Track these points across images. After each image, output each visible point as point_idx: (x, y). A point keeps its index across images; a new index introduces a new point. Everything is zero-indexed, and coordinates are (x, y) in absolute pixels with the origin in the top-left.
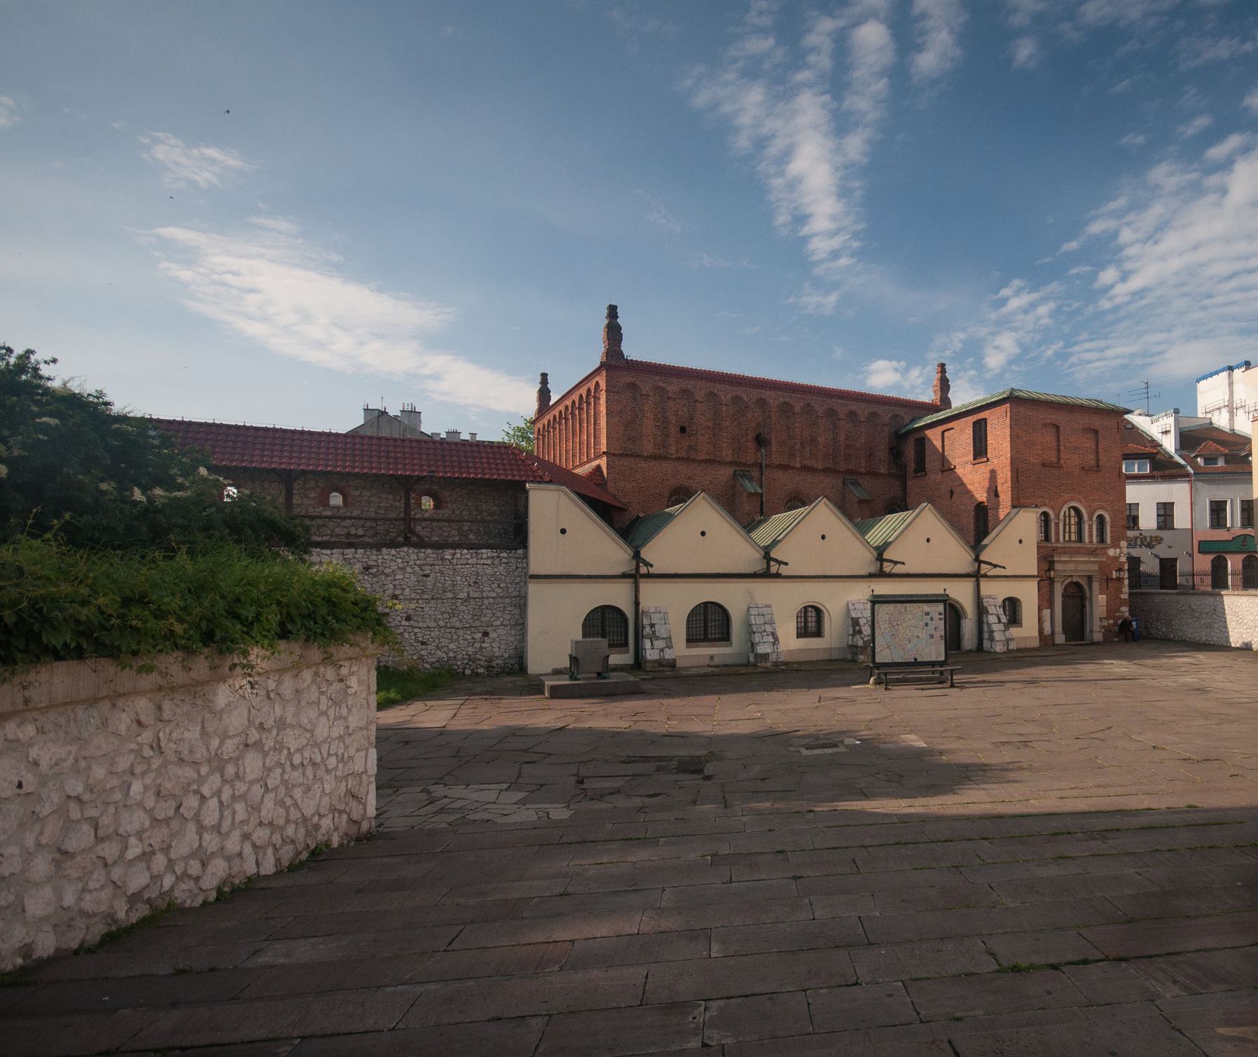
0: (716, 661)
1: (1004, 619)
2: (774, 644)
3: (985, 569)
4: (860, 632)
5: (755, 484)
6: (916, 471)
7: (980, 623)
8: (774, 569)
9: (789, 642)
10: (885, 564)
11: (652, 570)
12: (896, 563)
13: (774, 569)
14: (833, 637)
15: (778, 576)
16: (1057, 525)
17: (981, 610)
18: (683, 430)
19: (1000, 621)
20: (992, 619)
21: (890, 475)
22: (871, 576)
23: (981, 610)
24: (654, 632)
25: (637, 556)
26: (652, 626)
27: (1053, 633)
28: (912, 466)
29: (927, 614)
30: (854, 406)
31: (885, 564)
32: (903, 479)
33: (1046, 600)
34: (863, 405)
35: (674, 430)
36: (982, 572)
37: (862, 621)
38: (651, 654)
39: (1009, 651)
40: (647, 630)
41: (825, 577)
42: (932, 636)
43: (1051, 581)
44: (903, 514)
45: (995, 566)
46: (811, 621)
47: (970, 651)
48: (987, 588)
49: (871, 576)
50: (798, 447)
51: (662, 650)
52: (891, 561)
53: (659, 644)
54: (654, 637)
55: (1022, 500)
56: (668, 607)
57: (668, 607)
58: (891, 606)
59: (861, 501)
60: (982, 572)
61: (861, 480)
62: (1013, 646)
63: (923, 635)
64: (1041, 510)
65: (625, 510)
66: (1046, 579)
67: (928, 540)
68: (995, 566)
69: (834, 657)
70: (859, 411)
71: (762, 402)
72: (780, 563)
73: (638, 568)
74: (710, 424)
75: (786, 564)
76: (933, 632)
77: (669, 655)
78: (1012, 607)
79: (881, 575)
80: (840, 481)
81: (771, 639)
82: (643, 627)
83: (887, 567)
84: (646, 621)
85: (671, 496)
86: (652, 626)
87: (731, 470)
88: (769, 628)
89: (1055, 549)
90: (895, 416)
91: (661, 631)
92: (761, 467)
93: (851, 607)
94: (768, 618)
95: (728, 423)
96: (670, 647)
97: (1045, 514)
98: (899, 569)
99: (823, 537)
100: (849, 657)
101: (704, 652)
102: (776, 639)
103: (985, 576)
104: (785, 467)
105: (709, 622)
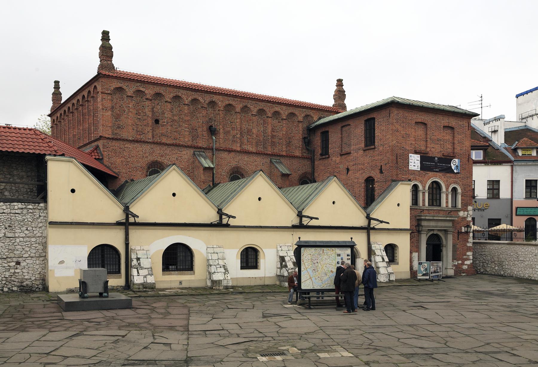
0: (184, 285)
1: (386, 259)
2: (225, 274)
3: (373, 223)
4: (286, 266)
5: (208, 161)
6: (322, 155)
8: (225, 221)
9: (236, 273)
10: (304, 219)
11: (138, 220)
12: (312, 218)
13: (225, 221)
14: (268, 268)
15: (227, 226)
16: (424, 193)
17: (370, 252)
18: (157, 122)
20: (378, 259)
21: (303, 158)
23: (370, 252)
24: (139, 264)
25: (126, 210)
26: (138, 259)
28: (319, 151)
29: (339, 255)
30: (277, 108)
31: (304, 219)
32: (312, 160)
33: (415, 247)
34: (284, 108)
35: (150, 122)
36: (372, 226)
37: (287, 259)
38: (137, 279)
40: (135, 262)
41: (261, 227)
43: (419, 232)
44: (310, 185)
45: (382, 222)
46: (250, 258)
49: (294, 227)
50: (238, 136)
51: (145, 277)
52: (308, 217)
53: (143, 272)
54: (139, 267)
56: (149, 249)
57: (149, 249)
59: (284, 175)
60: (372, 226)
61: (282, 160)
62: (393, 278)
65: (116, 178)
66: (416, 229)
67: (334, 203)
68: (382, 222)
69: (266, 283)
70: (281, 112)
71: (212, 104)
72: (230, 217)
73: (127, 218)
74: (175, 118)
75: (234, 217)
77: (150, 280)
78: (391, 249)
79: (300, 226)
80: (269, 162)
81: (222, 270)
82: (132, 260)
83: (305, 221)
84: (133, 256)
85: (149, 168)
86: (138, 259)
87: (192, 151)
88: (221, 263)
89: (423, 210)
90: (307, 116)
91: (145, 263)
92: (212, 149)
93: (279, 249)
94: (220, 255)
95: (189, 118)
96: (151, 275)
97: (415, 188)
98: (313, 223)
99: (260, 199)
100: (278, 283)
101: (175, 280)
102: (226, 270)
103: (374, 229)
104: (230, 151)
105: (177, 258)
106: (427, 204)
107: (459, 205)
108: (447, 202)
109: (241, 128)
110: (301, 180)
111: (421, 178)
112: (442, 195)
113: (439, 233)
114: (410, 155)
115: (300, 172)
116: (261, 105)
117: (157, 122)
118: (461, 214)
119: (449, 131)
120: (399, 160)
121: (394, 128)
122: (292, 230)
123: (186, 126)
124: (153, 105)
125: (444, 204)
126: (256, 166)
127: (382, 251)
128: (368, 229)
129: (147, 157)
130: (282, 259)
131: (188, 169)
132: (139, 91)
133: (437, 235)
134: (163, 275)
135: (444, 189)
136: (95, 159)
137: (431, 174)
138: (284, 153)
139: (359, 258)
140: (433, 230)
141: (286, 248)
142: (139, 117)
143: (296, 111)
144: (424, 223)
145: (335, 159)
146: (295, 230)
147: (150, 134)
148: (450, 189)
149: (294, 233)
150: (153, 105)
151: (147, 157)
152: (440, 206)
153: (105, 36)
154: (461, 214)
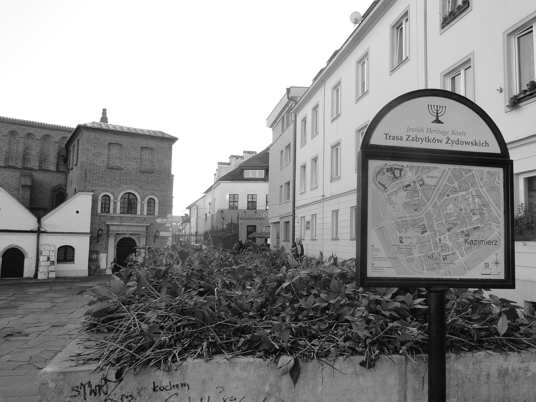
1: (54, 258)
7: (38, 260)
16: (115, 203)
19: (48, 259)
34: (39, 130)
39: (49, 278)
47: (29, 278)
48: (44, 239)
55: (88, 188)
61: (34, 174)
62: (53, 275)
64: (103, 194)
106: (118, 211)
108: (142, 210)
110: (55, 191)
111: (113, 190)
113: (132, 237)
115: (54, 184)
116: (13, 128)
118: (159, 221)
119: (149, 151)
120: (88, 174)
121: (84, 148)
125: (139, 212)
126: (4, 178)
127: (51, 252)
128: (39, 232)
137: (124, 186)
138: (37, 168)
143: (52, 133)
144: (111, 228)
145: (70, 173)
148: (146, 200)
152: (136, 213)
154: (159, 221)
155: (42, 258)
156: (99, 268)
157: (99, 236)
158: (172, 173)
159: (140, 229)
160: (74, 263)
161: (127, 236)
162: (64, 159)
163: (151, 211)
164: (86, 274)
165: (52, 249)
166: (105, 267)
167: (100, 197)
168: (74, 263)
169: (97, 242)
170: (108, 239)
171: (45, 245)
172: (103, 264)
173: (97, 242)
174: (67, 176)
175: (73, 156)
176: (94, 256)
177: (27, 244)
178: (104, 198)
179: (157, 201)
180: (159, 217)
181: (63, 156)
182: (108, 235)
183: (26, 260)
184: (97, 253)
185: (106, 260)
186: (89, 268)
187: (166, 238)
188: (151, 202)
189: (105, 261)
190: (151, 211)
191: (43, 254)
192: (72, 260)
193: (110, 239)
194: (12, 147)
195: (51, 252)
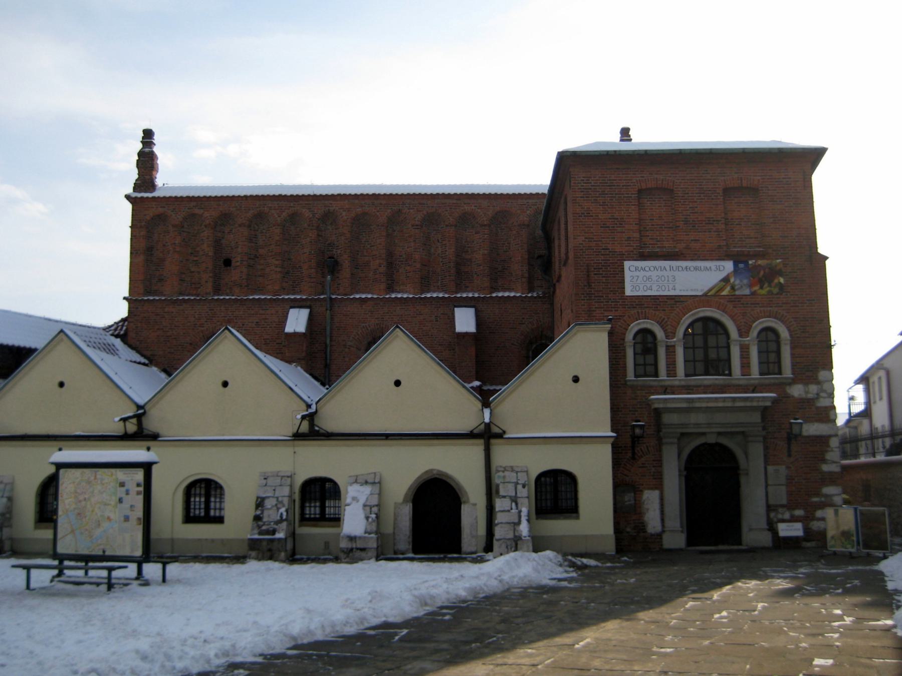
16: (670, 350)
22: (298, 436)
27: (663, 531)
37: (269, 503)
42: (127, 519)
49: (298, 436)
58: (77, 472)
63: (116, 515)
64: (634, 327)
74: (261, 251)
76: (128, 513)
107: (787, 372)
108: (746, 366)
109: (390, 254)
112: (732, 347)
113: (724, 441)
114: (627, 264)
117: (228, 263)
118: (797, 391)
122: (291, 443)
123: (277, 262)
124: (219, 234)
127: (520, 487)
128: (488, 435)
129: (201, 325)
130: (260, 503)
131: (278, 341)
132: (194, 215)
133: (717, 444)
134: (36, 528)
135: (734, 333)
136: (112, 335)
139: (465, 502)
140: (704, 434)
141: (278, 481)
142: (195, 259)
144: (667, 419)
146: (297, 443)
147: (210, 285)
148: (754, 333)
149: (297, 449)
150: (219, 234)
151: (201, 325)
152: (730, 374)
153: (148, 135)
154: (797, 391)
155: (499, 504)
156: (645, 531)
157: (635, 440)
158: (822, 249)
159: (743, 418)
160: (578, 518)
161: (712, 440)
162: (543, 264)
163: (771, 363)
164: (610, 547)
165: (523, 478)
166: (659, 529)
167: (629, 336)
168: (578, 518)
169: (633, 458)
170: (660, 450)
171: (505, 469)
172: (653, 522)
173: (633, 458)
174: (552, 304)
175: (559, 246)
176: (629, 498)
177: (462, 465)
178: (639, 338)
179: (784, 333)
180: (793, 382)
181: (540, 257)
182: (660, 440)
183: (465, 510)
184: (636, 490)
185: (663, 509)
186: (617, 530)
187: (822, 441)
188: (769, 337)
189: (658, 512)
190: (771, 363)
191: (502, 493)
192: (571, 509)
193: (665, 449)
194: (432, 250)
195: (520, 487)
